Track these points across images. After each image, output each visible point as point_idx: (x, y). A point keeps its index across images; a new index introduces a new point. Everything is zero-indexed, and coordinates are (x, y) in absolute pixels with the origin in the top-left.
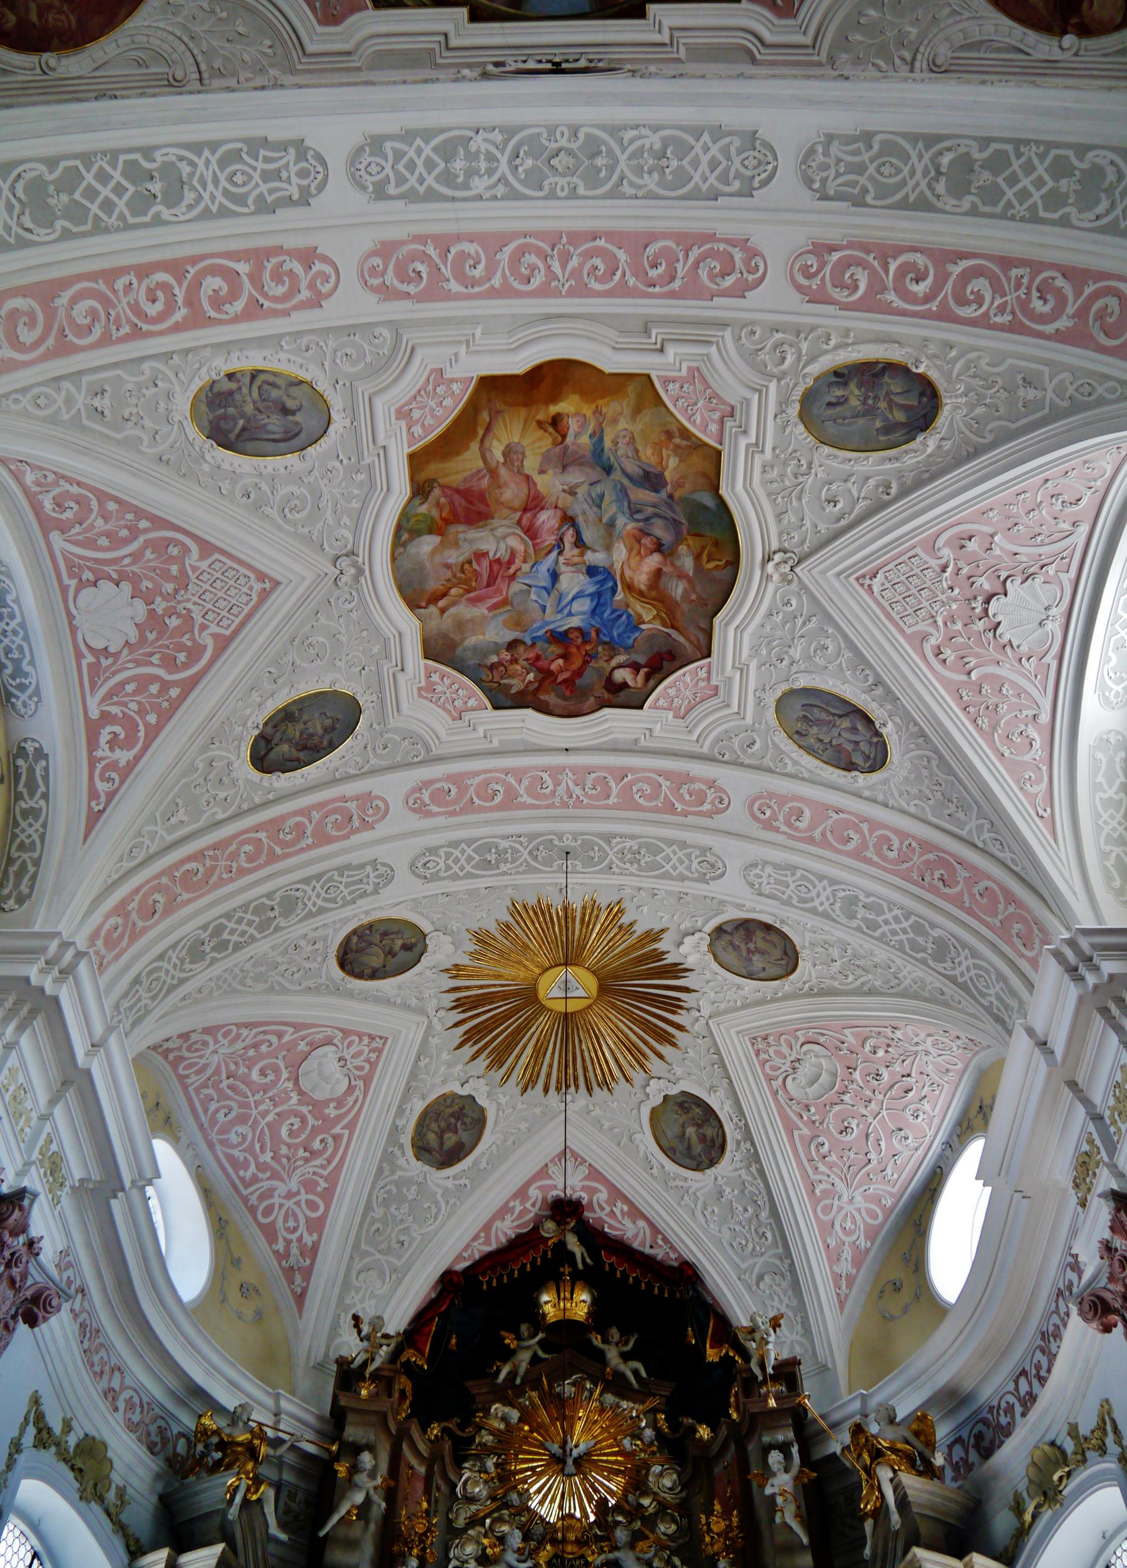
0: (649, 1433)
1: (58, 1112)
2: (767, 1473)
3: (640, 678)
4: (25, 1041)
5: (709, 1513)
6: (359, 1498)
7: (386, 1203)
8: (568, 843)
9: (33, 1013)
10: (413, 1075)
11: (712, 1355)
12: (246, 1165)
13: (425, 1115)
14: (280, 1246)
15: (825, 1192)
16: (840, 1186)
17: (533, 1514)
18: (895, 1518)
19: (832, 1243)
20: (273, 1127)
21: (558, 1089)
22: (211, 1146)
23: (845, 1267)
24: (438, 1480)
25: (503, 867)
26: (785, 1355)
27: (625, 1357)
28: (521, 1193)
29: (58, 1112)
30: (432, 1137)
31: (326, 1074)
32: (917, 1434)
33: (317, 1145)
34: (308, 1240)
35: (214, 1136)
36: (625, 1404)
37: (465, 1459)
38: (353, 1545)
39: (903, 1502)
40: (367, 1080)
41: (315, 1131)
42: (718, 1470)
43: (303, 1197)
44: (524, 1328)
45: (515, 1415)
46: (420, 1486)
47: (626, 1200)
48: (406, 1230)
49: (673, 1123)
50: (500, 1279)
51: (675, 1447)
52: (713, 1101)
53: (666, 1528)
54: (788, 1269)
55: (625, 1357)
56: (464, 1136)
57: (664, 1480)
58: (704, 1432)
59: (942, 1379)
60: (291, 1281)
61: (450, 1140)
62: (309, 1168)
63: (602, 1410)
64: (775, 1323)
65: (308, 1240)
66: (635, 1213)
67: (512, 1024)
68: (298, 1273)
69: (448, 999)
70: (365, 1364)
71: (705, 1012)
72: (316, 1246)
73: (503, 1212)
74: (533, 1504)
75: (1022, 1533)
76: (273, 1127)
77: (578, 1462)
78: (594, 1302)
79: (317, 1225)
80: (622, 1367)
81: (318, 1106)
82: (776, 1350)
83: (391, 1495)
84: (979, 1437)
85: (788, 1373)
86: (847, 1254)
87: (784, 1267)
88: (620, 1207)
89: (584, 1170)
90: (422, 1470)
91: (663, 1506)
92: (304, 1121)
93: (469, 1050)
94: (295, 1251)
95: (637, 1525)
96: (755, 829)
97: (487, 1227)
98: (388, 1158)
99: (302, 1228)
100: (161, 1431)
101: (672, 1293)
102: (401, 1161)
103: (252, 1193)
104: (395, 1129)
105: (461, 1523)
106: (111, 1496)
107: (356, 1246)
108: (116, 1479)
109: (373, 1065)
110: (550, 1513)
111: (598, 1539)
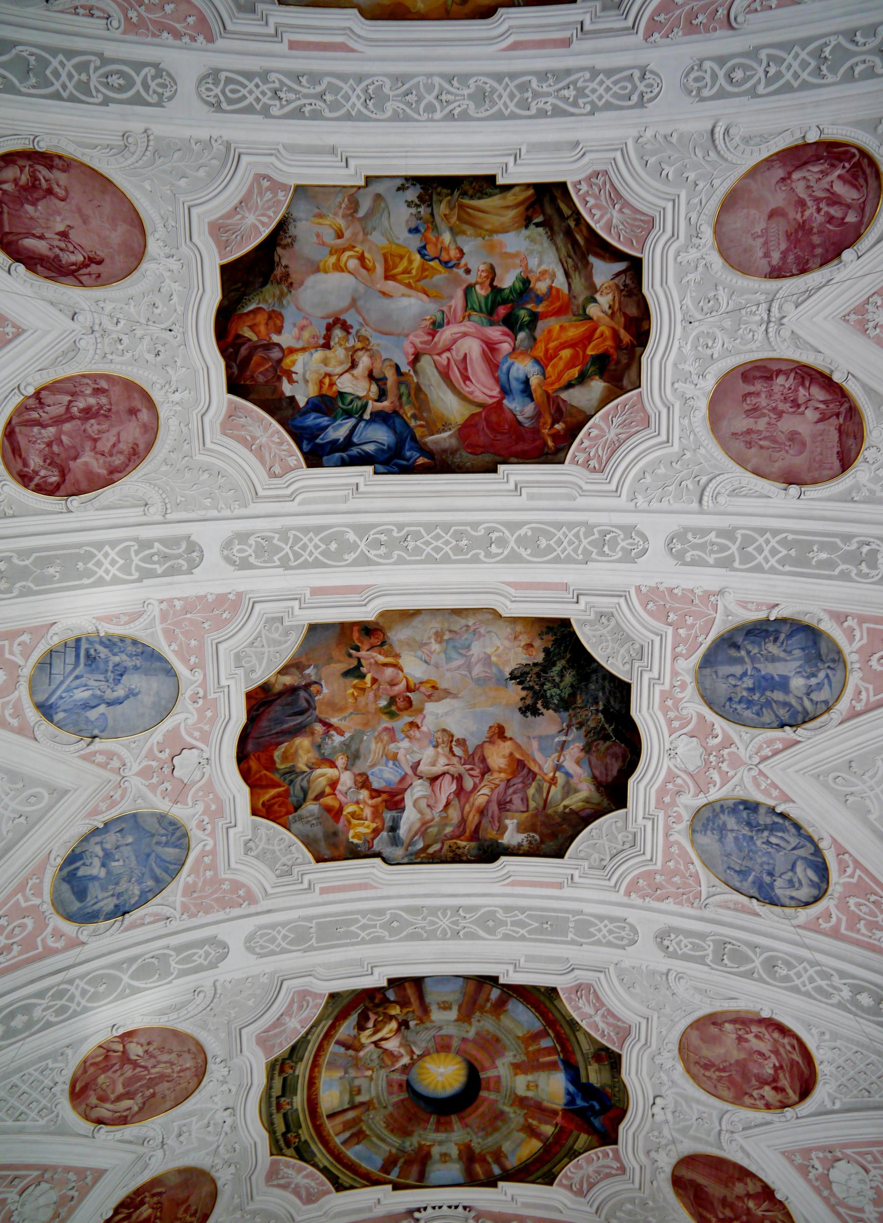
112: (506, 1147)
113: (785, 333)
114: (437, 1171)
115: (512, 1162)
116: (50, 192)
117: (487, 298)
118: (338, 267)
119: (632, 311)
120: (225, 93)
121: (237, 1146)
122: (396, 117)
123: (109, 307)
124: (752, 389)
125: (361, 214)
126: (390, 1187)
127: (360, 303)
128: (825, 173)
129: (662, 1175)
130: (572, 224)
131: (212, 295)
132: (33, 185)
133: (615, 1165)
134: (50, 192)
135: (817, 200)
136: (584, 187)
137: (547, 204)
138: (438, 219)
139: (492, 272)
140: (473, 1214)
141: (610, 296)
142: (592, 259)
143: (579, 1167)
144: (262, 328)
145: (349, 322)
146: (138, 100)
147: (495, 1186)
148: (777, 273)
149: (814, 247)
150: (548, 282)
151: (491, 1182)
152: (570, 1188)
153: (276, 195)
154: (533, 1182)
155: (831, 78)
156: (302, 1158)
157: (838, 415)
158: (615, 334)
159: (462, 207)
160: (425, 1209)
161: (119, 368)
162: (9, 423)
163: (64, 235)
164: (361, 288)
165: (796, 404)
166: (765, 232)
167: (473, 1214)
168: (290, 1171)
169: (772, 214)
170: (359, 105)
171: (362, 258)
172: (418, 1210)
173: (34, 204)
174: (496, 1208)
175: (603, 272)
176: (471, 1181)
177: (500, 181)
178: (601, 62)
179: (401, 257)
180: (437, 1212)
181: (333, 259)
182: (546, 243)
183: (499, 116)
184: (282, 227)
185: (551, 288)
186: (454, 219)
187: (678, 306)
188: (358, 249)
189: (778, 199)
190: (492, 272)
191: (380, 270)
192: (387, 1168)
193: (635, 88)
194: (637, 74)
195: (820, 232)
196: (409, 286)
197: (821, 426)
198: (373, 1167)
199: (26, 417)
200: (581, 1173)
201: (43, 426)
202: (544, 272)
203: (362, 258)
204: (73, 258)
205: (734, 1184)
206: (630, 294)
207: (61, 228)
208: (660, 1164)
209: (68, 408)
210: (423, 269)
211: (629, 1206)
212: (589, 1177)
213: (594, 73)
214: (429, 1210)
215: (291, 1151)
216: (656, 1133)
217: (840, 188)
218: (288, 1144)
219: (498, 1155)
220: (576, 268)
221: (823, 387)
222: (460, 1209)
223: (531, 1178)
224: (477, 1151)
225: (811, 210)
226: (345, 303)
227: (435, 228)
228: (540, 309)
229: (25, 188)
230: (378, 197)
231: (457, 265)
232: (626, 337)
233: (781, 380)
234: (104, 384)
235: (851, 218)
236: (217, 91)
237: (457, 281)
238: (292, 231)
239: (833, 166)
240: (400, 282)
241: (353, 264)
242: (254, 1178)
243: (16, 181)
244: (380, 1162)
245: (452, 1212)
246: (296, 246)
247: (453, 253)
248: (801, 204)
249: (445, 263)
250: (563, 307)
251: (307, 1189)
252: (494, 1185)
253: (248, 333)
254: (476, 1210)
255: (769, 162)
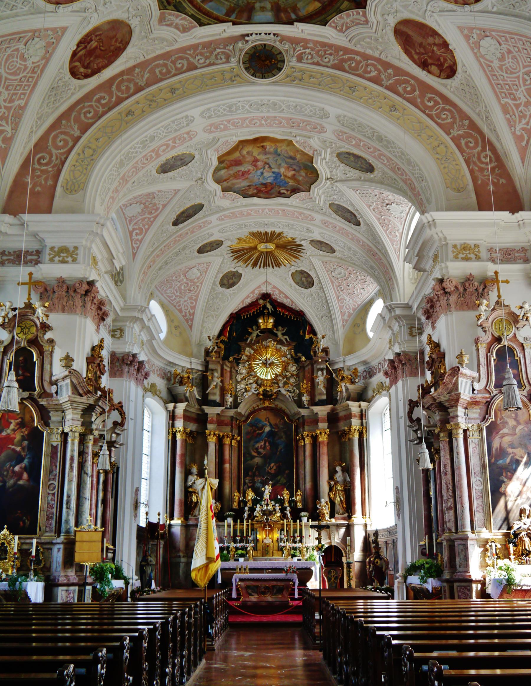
0: (289, 356)
1: (142, 333)
2: (317, 377)
3: (289, 192)
4: (135, 326)
5: (303, 382)
6: (215, 383)
7: (213, 299)
8: (266, 223)
9: (136, 320)
10: (219, 268)
11: (307, 337)
12: (172, 296)
13: (223, 277)
14: (184, 314)
15: (342, 299)
16: (346, 298)
17: (259, 377)
18: (344, 394)
19: (343, 311)
20: (180, 288)
21: (264, 267)
22: (162, 295)
23: (346, 317)
24: (233, 371)
25: (239, 111)
26: (325, 346)
27: (283, 334)
28: (253, 292)
29: (142, 333)
30: (225, 282)
31: (195, 273)
32: (354, 373)
33: (192, 288)
34: (191, 311)
35: (163, 292)
36: (283, 348)
37: (239, 363)
38: (214, 394)
39: (347, 389)
40: (206, 272)
41: (191, 286)
42: (306, 369)
43: (189, 301)
44: (254, 327)
45: (252, 352)
46: (228, 374)
47: (284, 294)
48: (219, 305)
49: (298, 277)
50: (247, 316)
51: (297, 360)
52: (311, 273)
53: (292, 380)
54: (329, 315)
55: (283, 334)
56: (235, 280)
57: (293, 368)
58: (303, 359)
59: (363, 359)
60: (188, 322)
61: (231, 281)
62: (190, 294)
63: (276, 350)
64: (323, 337)
65: (191, 311)
66: (287, 297)
67: (249, 254)
68: (189, 320)
69: (230, 252)
70: (213, 349)
71: (308, 254)
72: (194, 313)
73: (248, 296)
74: (258, 375)
75: (373, 397)
76: (180, 288)
77: (270, 364)
78: (275, 321)
79: (194, 308)
80: (282, 338)
81: (191, 281)
82: (323, 344)
83: (222, 381)
84: (370, 372)
85: (326, 351)
86: (347, 314)
87: (329, 315)
88: (282, 295)
89: (271, 286)
90: (229, 369)
91: (292, 375)
92: (188, 284)
93: (236, 261)
94: (188, 315)
95: (285, 380)
96: (322, 226)
97: (243, 302)
98: (212, 288)
99: (189, 309)
100: (164, 373)
101: (297, 318)
102: (217, 288)
103: (175, 303)
104: (214, 281)
105: (239, 379)
106: (158, 393)
107: (205, 311)
108: (158, 388)
109: (207, 269)
110: (263, 377)
111: (275, 383)
112: (300, 5)
114: (258, 16)
115: (303, 13)
121: (139, 7)
126: (231, 24)
129: (389, 27)
133: (363, 19)
140: (279, 38)
143: (341, 18)
147: (293, 24)
151: (290, 23)
152: (336, 28)
154: (314, 24)
156: (178, 11)
160: (252, 34)
167: (279, 38)
168: (172, 17)
172: (247, 35)
174: (292, 35)
176: (278, 21)
180: (259, 37)
192: (228, 14)
198: (221, 14)
200: (342, 21)
205: (428, 37)
208: (389, 21)
211: (368, 40)
212: (347, 23)
214: (254, 35)
215: (172, 7)
216: (389, 6)
218: (169, 3)
219: (295, 9)
222: (272, 35)
223: (314, 21)
224: (282, 6)
242: (151, 23)
244: (224, 11)
245: (267, 37)
251: (183, 26)
252: (292, 24)
254: (281, 36)
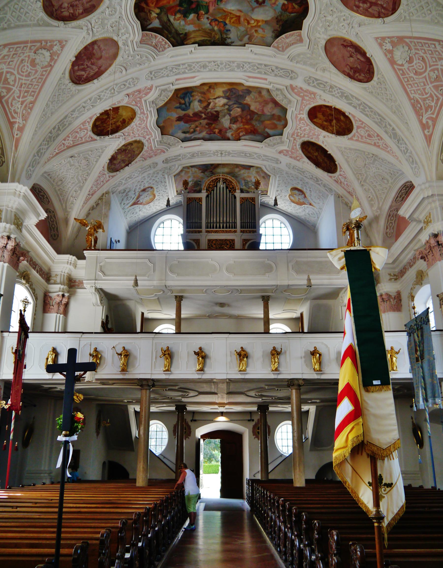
113: (85, 28)
116: (351, 68)
117: (200, 10)
118: (258, 21)
119: (142, 14)
120: (290, 74)
122: (233, 62)
123: (344, 31)
124: (90, 4)
125: (248, 36)
127: (250, 9)
128: (89, 74)
130: (169, 36)
131: (307, 22)
132: (355, 72)
134: (351, 68)
135: (88, 67)
136: (167, 46)
137: (179, 40)
138: (219, 33)
139: (198, 18)
141: (152, 16)
142: (161, 27)
144: (290, 6)
145: (255, 3)
146: (317, 80)
148: (93, 43)
149: (85, 55)
150: (176, 17)
153: (278, 45)
155: (96, 96)
157: (56, 10)
158: (147, 5)
159: (210, 37)
161: (347, 12)
162: (392, 14)
163: (351, 56)
164: (250, 14)
165: (72, 6)
166: (101, 52)
169: (101, 57)
170: (246, 65)
171: (249, 23)
173: (357, 68)
175: (156, 23)
177: (197, 45)
178: (166, 78)
179: (233, 22)
181: (259, 24)
182: (178, 29)
183: (198, 63)
184: (277, 36)
185: (175, 15)
186: (213, 33)
187: (125, 20)
188: (249, 26)
189: (100, 62)
190: (198, 18)
191: (242, 19)
193: (154, 75)
194: (154, 78)
195: (84, 60)
196: (231, 13)
197: (60, 3)
199: (386, 12)
201: (382, 6)
202: (178, 20)
203: (249, 23)
204: (351, 49)
206: (144, 19)
207: (351, 59)
209: (370, 7)
210: (225, 19)
213: (168, 76)
217: (83, 73)
220: (166, 23)
221: (65, 16)
225: (89, 64)
226: (256, 10)
227: (220, 31)
228: (178, 8)
229: (358, 72)
230: (241, 40)
231: (212, 20)
232: (144, 5)
233: (81, 11)
234: (355, 8)
235: (76, 68)
236: (291, 75)
237: (212, 15)
238: (274, 35)
239: (87, 77)
240: (234, 15)
241: (252, 22)
243: (360, 75)
246: (273, 29)
247: (213, 24)
248: (93, 64)
249: (216, 20)
250: (169, 10)
253: (296, 6)
255: (106, 70)
